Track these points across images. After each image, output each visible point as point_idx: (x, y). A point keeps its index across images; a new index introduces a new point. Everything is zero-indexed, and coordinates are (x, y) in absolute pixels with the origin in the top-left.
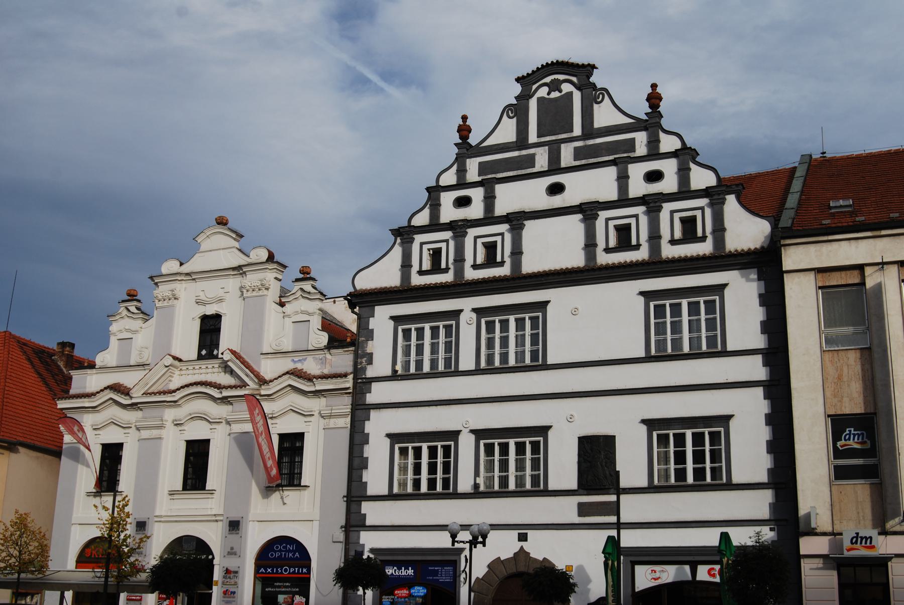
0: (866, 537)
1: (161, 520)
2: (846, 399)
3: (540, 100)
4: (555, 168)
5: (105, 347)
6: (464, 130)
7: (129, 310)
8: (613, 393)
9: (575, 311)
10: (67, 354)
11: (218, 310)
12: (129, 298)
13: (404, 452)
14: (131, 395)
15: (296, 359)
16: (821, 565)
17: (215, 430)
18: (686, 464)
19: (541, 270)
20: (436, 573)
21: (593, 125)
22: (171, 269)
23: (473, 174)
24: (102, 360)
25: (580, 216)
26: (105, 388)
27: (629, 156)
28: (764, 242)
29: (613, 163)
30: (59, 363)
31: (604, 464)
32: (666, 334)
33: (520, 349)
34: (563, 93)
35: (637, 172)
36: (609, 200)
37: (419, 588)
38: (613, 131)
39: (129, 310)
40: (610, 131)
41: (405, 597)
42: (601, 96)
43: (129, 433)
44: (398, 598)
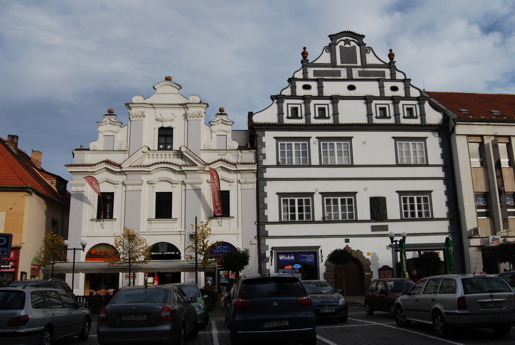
0: (497, 239)
2: (479, 186)
3: (341, 47)
4: (350, 78)
5: (96, 139)
6: (305, 54)
7: (110, 120)
8: (350, 179)
9: (365, 142)
10: (16, 142)
11: (170, 125)
12: (109, 113)
13: (285, 201)
14: (122, 166)
15: (221, 154)
16: (476, 250)
17: (175, 188)
18: (295, 212)
20: (305, 258)
22: (138, 100)
23: (311, 75)
25: (364, 101)
26: (103, 162)
27: (324, 78)
28: (440, 122)
29: (378, 80)
30: (10, 147)
31: (383, 209)
32: (334, 156)
33: (289, 158)
35: (388, 85)
36: (345, 96)
37: (297, 265)
38: (328, 66)
39: (110, 120)
40: (374, 66)
41: (290, 270)
42: (369, 50)
43: (175, 187)
44: (287, 270)
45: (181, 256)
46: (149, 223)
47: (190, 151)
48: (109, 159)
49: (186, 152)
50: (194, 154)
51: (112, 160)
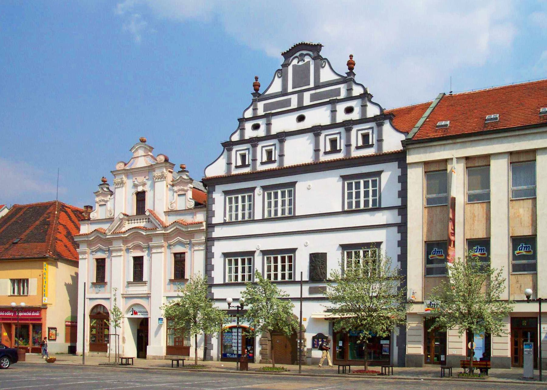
4: (301, 107)
6: (256, 86)
19: (296, 164)
21: (320, 81)
34: (305, 62)
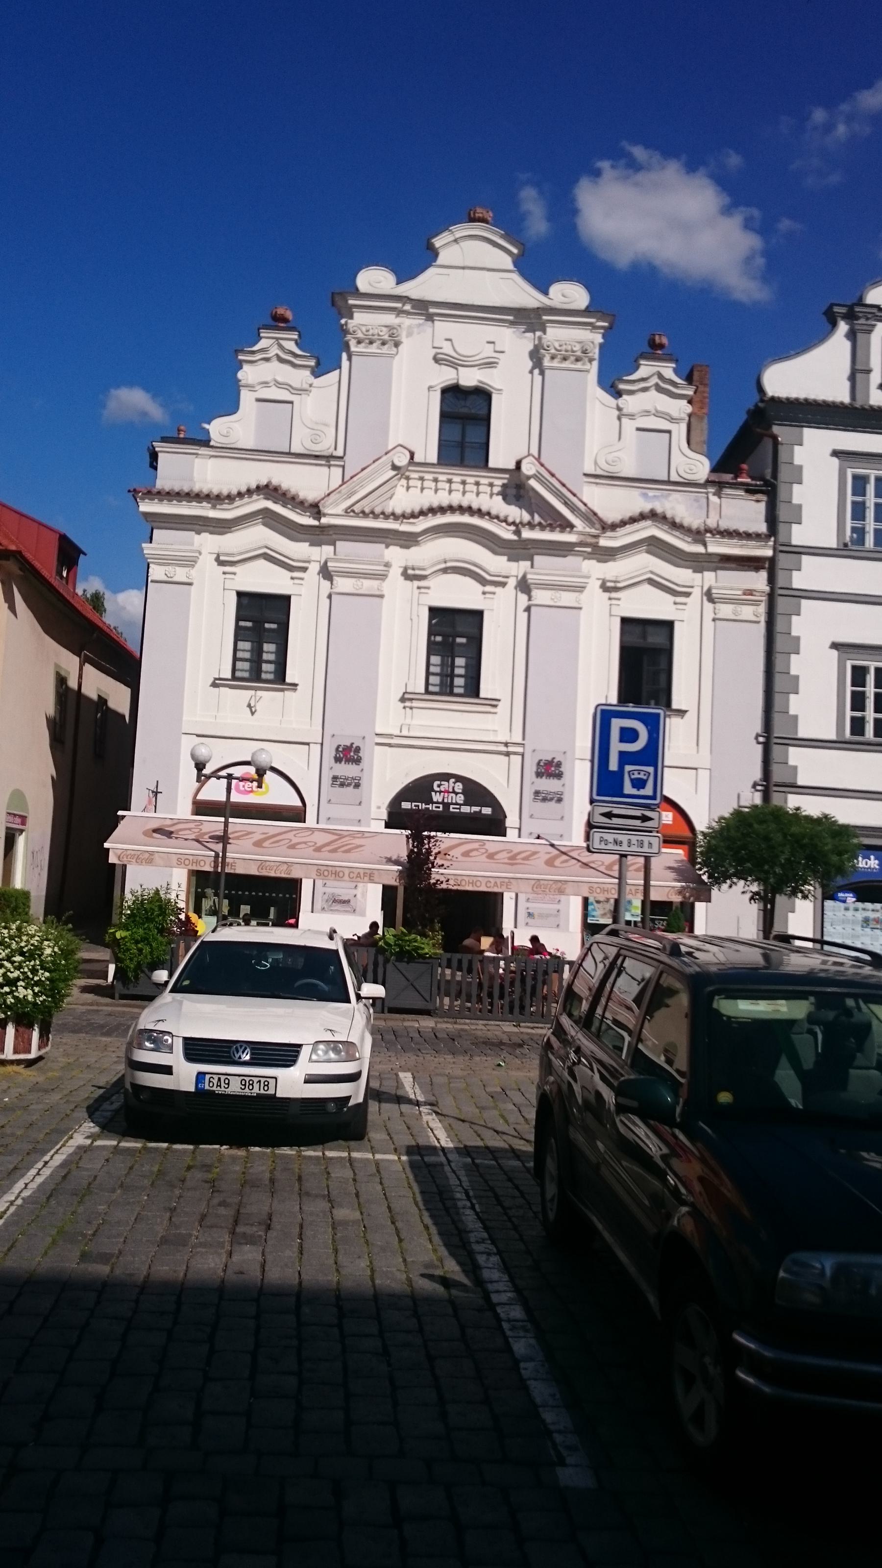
1: (387, 742)
5: (231, 407)
7: (281, 347)
14: (321, 508)
15: (651, 493)
24: (224, 433)
39: (281, 347)
45: (508, 823)
46: (404, 708)
47: (553, 475)
48: (275, 482)
49: (534, 476)
50: (564, 485)
51: (285, 486)
